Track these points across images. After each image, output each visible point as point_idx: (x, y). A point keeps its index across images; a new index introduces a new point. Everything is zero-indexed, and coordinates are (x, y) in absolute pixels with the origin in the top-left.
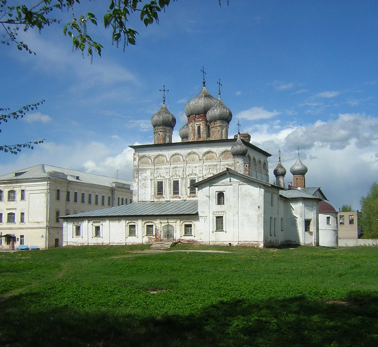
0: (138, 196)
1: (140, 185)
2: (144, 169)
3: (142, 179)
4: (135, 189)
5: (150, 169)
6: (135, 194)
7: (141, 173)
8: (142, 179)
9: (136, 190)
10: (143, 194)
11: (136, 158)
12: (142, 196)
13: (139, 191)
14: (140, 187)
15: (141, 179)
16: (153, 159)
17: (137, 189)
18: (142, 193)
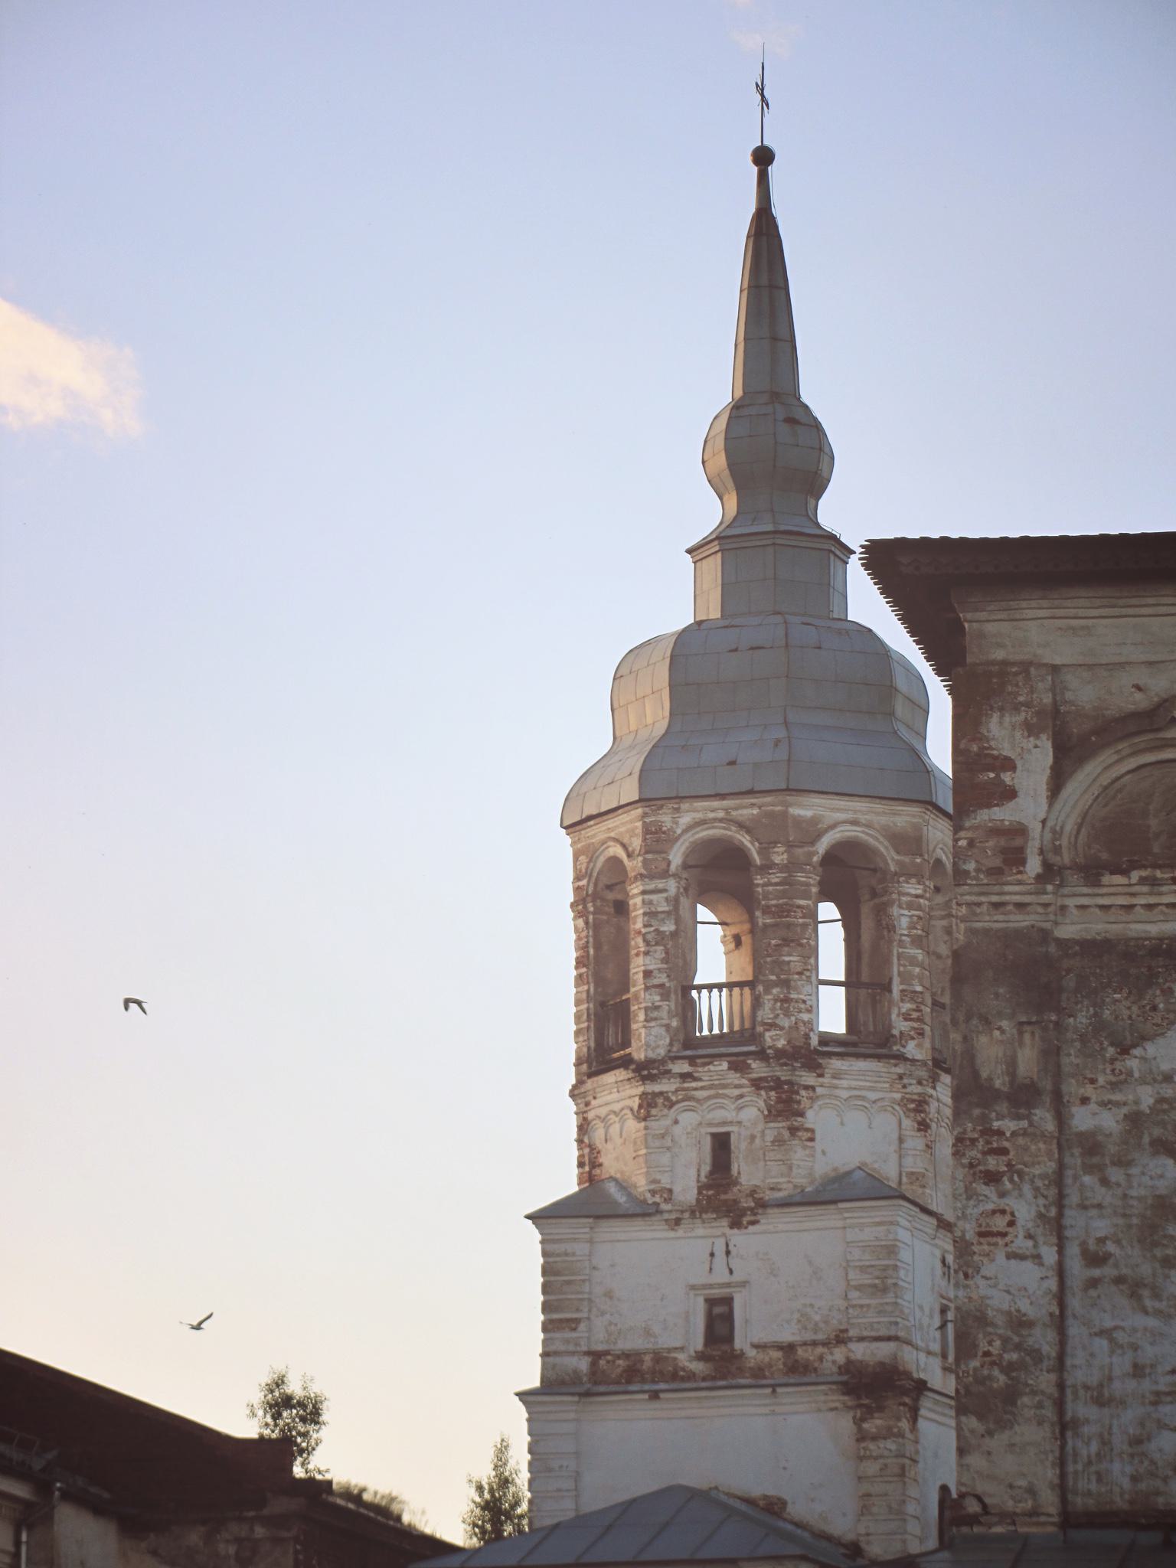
0: (1064, 1426)
1: (1101, 1226)
3: (1135, 1120)
4: (998, 1301)
6: (1010, 1396)
7: (1099, 1026)
8: (1135, 1120)
9: (1020, 1323)
10: (1157, 1399)
11: (1009, 765)
12: (1129, 1416)
13: (1074, 1330)
14: (1094, 1259)
15: (1109, 1122)
17: (1036, 1303)
18: (1138, 1371)
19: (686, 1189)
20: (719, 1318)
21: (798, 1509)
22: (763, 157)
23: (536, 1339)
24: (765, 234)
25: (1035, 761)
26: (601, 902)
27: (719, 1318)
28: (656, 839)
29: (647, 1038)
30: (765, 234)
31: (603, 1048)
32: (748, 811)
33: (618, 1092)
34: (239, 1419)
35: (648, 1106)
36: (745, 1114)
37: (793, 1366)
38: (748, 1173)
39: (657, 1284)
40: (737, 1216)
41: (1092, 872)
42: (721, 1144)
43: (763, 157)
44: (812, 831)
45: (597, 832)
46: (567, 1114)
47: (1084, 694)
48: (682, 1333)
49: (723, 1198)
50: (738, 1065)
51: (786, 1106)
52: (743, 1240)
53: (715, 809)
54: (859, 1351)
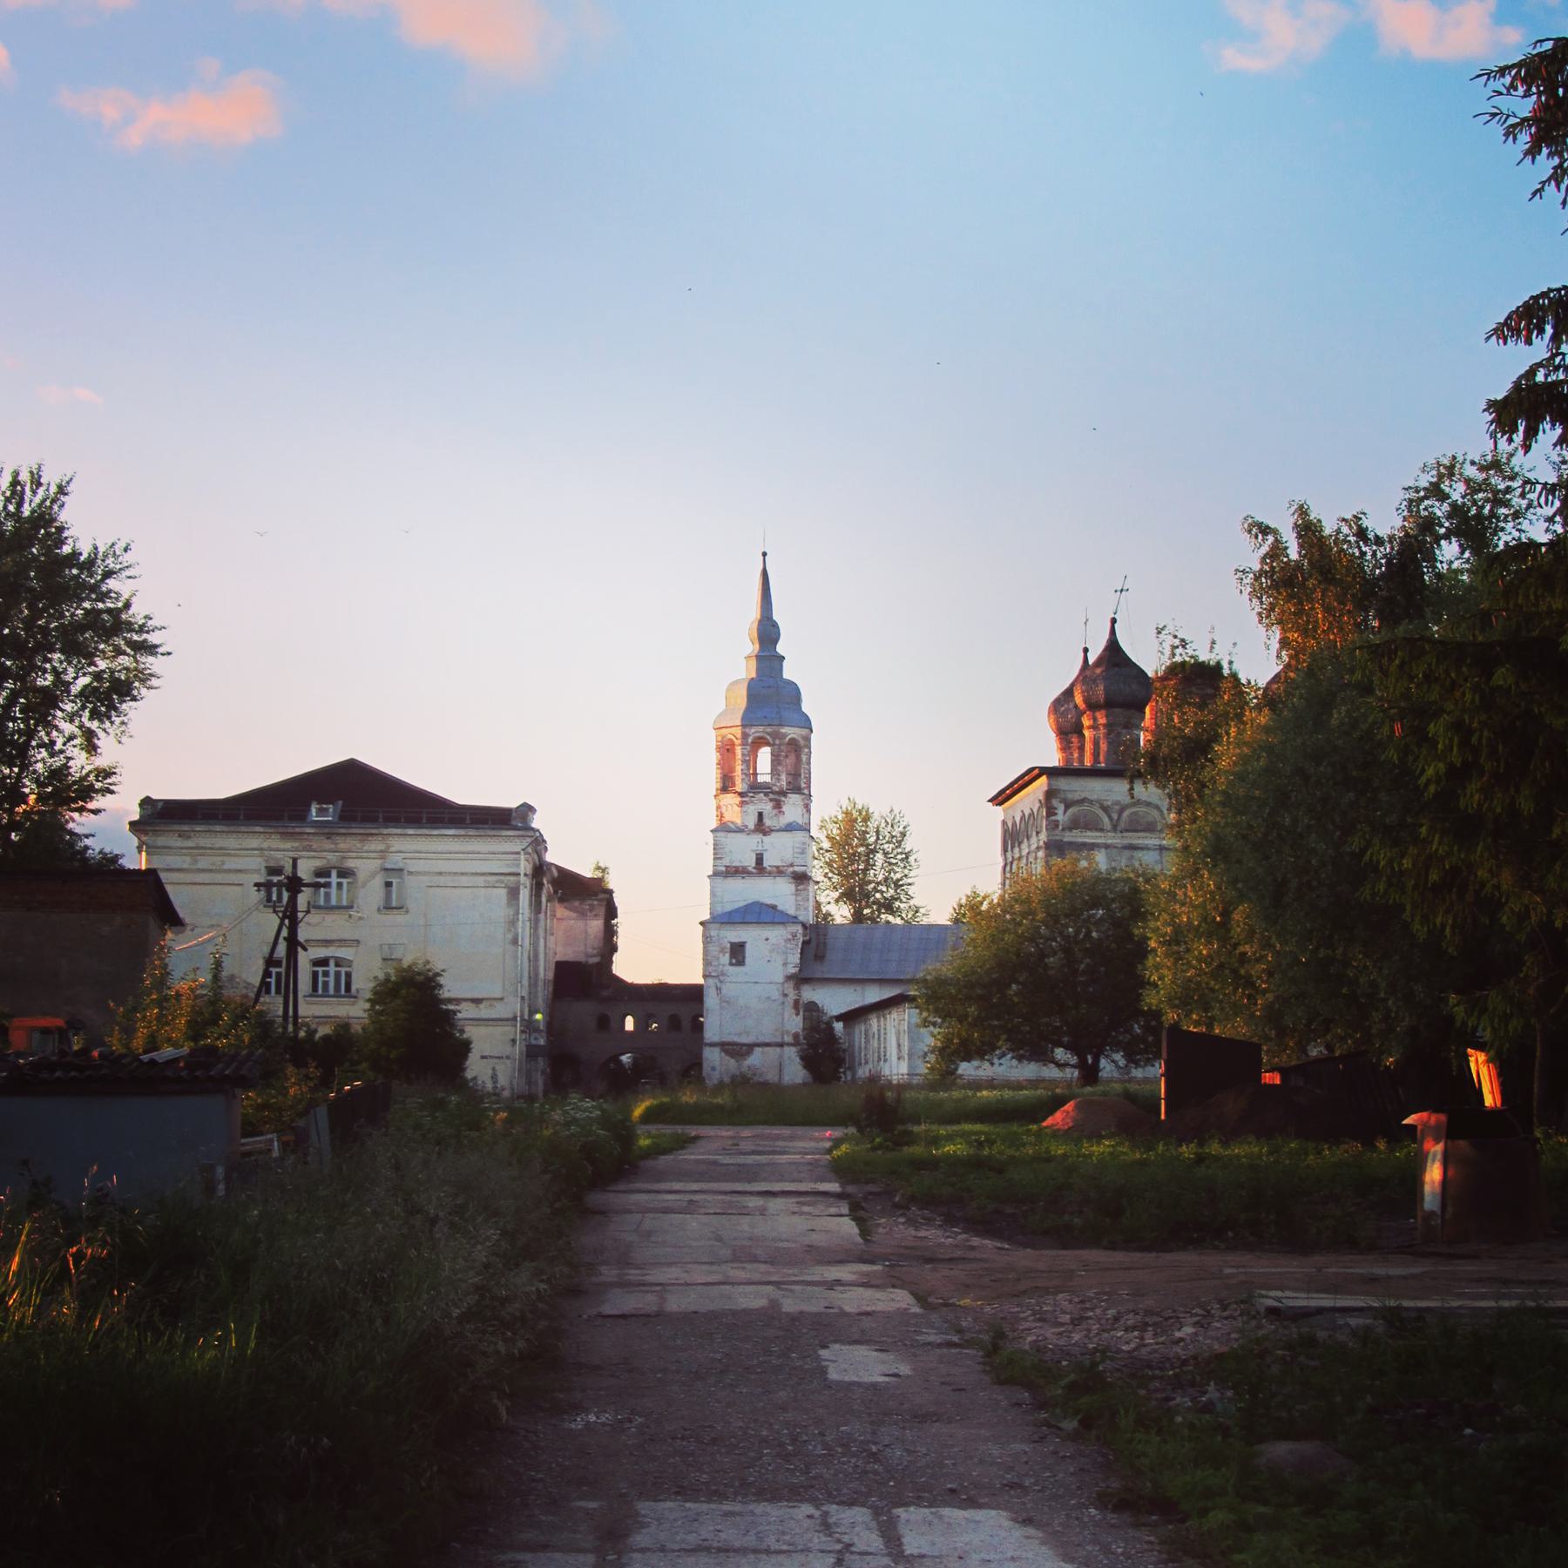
2: (1084, 845)
5: (1107, 846)
16: (1115, 816)
19: (751, 826)
20: (760, 859)
21: (780, 908)
22: (764, 554)
23: (711, 862)
24: (765, 574)
25: (1061, 808)
26: (726, 749)
27: (760, 859)
28: (745, 736)
29: (740, 786)
30: (765, 574)
31: (726, 785)
32: (769, 730)
33: (731, 800)
34: (587, 872)
35: (742, 804)
36: (767, 807)
37: (779, 872)
38: (767, 822)
39: (743, 850)
40: (765, 833)
41: (1070, 829)
42: (760, 815)
43: (764, 554)
44: (785, 735)
45: (724, 731)
46: (714, 803)
47: (1070, 796)
48: (751, 863)
49: (761, 827)
50: (766, 794)
51: (778, 805)
52: (766, 839)
53: (761, 729)
54: (797, 869)
